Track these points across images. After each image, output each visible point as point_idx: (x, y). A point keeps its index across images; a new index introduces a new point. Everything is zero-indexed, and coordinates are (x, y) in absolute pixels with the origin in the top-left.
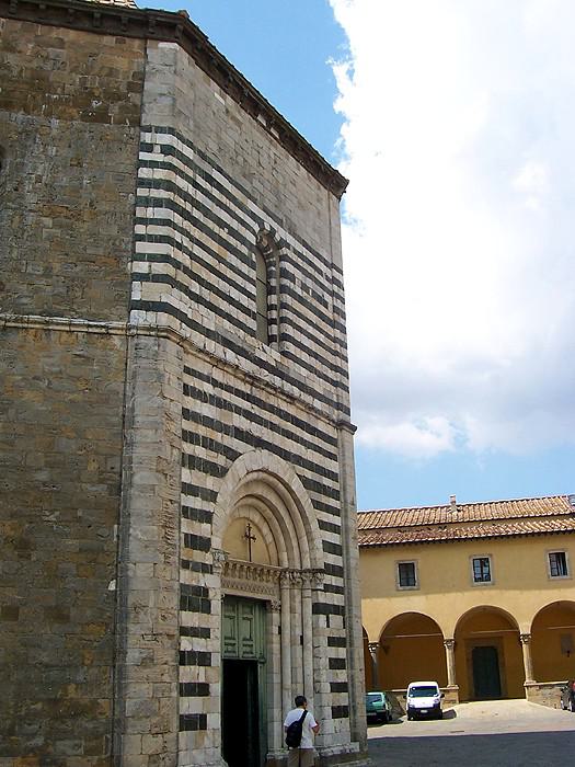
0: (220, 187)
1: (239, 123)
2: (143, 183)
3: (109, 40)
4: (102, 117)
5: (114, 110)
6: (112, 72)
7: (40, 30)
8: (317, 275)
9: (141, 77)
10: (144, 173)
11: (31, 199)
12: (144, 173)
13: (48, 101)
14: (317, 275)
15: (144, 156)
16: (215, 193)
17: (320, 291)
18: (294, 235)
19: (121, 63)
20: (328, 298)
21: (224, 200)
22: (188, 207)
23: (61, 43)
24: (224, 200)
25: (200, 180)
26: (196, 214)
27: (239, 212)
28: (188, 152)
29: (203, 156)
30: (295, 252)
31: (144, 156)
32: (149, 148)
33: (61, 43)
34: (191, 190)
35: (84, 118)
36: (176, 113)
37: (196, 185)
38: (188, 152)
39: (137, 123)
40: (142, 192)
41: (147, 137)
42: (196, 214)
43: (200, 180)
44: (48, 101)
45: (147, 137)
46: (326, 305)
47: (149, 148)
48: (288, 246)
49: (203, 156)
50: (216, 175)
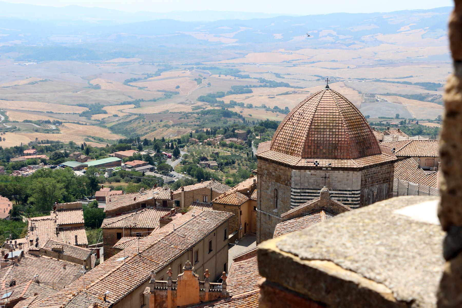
0: (308, 193)
1: (315, 175)
2: (292, 198)
5: (288, 184)
7: (279, 166)
8: (344, 196)
10: (292, 196)
12: (292, 196)
13: (281, 181)
14: (344, 196)
16: (307, 194)
17: (345, 199)
18: (335, 190)
19: (289, 174)
20: (348, 199)
21: (310, 194)
22: (299, 201)
23: (282, 169)
24: (310, 194)
25: (302, 194)
26: (301, 201)
27: (315, 195)
28: (299, 191)
29: (303, 189)
30: (335, 194)
31: (292, 193)
32: (292, 191)
33: (282, 169)
34: (299, 197)
35: (285, 185)
36: (296, 184)
37: (301, 196)
38: (299, 191)
40: (291, 200)
42: (301, 201)
43: (302, 194)
44: (281, 181)
46: (348, 201)
48: (333, 194)
49: (303, 189)
50: (307, 191)
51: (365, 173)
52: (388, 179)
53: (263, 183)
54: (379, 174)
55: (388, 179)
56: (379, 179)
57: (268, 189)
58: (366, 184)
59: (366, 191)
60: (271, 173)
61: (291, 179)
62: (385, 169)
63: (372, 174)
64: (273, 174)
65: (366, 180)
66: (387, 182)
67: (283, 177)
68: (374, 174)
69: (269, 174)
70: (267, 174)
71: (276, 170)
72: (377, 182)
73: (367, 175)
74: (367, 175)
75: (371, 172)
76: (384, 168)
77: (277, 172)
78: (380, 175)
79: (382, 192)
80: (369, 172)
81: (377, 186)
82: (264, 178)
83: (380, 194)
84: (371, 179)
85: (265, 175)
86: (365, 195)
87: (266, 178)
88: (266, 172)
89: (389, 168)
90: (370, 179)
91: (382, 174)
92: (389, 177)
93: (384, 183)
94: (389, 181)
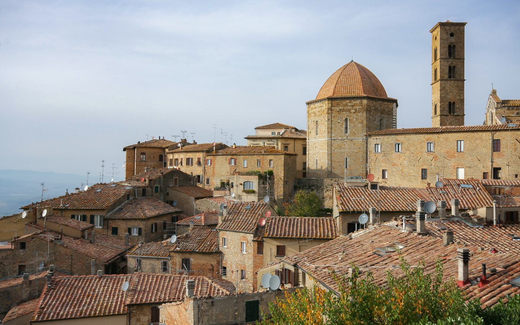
3: (390, 103)
4: (389, 115)
5: (390, 114)
6: (390, 108)
9: (393, 108)
11: (385, 126)
15: (393, 120)
19: (391, 107)
23: (385, 104)
32: (393, 118)
33: (385, 104)
39: (392, 115)
40: (393, 124)
41: (393, 117)
45: (393, 117)
47: (393, 118)
53: (371, 117)
57: (374, 121)
60: (377, 108)
61: (392, 110)
64: (379, 108)
67: (387, 110)
69: (376, 109)
70: (374, 110)
71: (381, 106)
77: (382, 107)
82: (372, 113)
85: (373, 111)
87: (373, 113)
88: (373, 108)
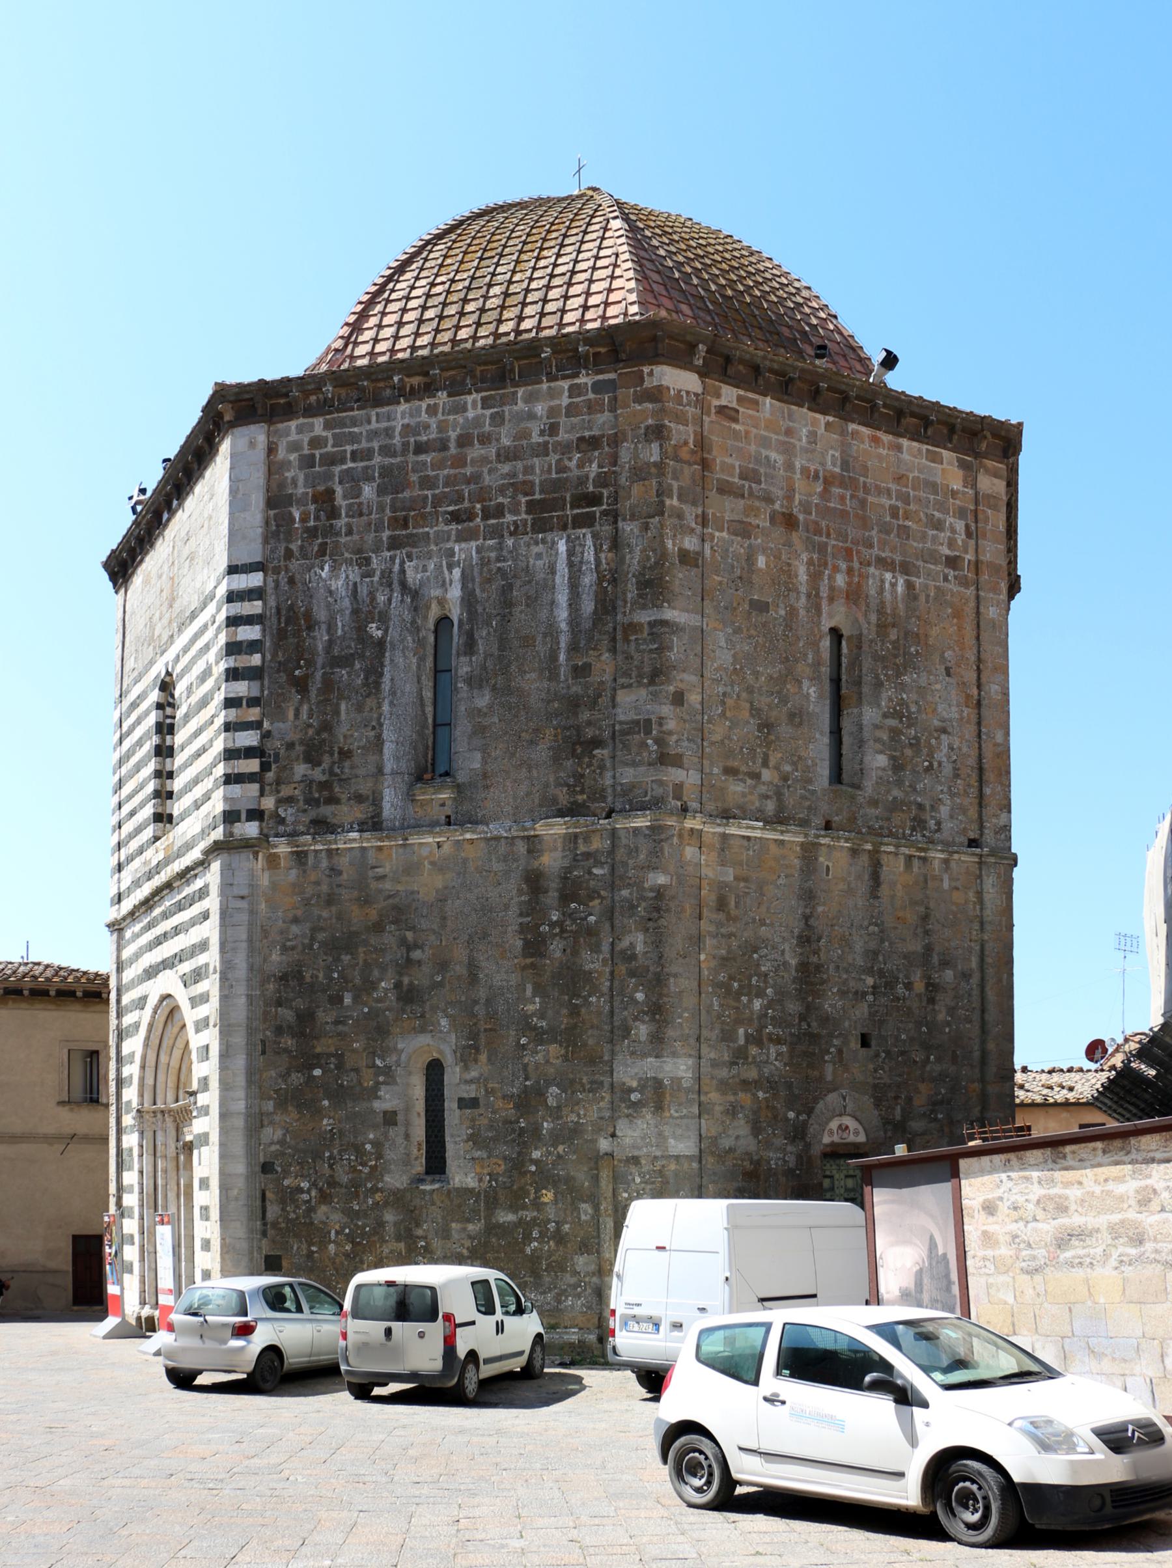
51: (316, 442)
52: (595, 500)
54: (476, 451)
55: (595, 500)
56: (482, 495)
58: (331, 531)
59: (338, 584)
62: (552, 412)
63: (386, 450)
65: (325, 499)
66: (585, 521)
68: (420, 449)
72: (455, 517)
73: (332, 460)
74: (332, 460)
75: (373, 435)
76: (540, 409)
78: (485, 460)
79: (532, 601)
80: (354, 438)
81: (467, 551)
83: (505, 619)
84: (381, 491)
86: (321, 615)
89: (592, 407)
90: (368, 491)
91: (506, 455)
92: (602, 480)
93: (541, 526)
94: (614, 516)
